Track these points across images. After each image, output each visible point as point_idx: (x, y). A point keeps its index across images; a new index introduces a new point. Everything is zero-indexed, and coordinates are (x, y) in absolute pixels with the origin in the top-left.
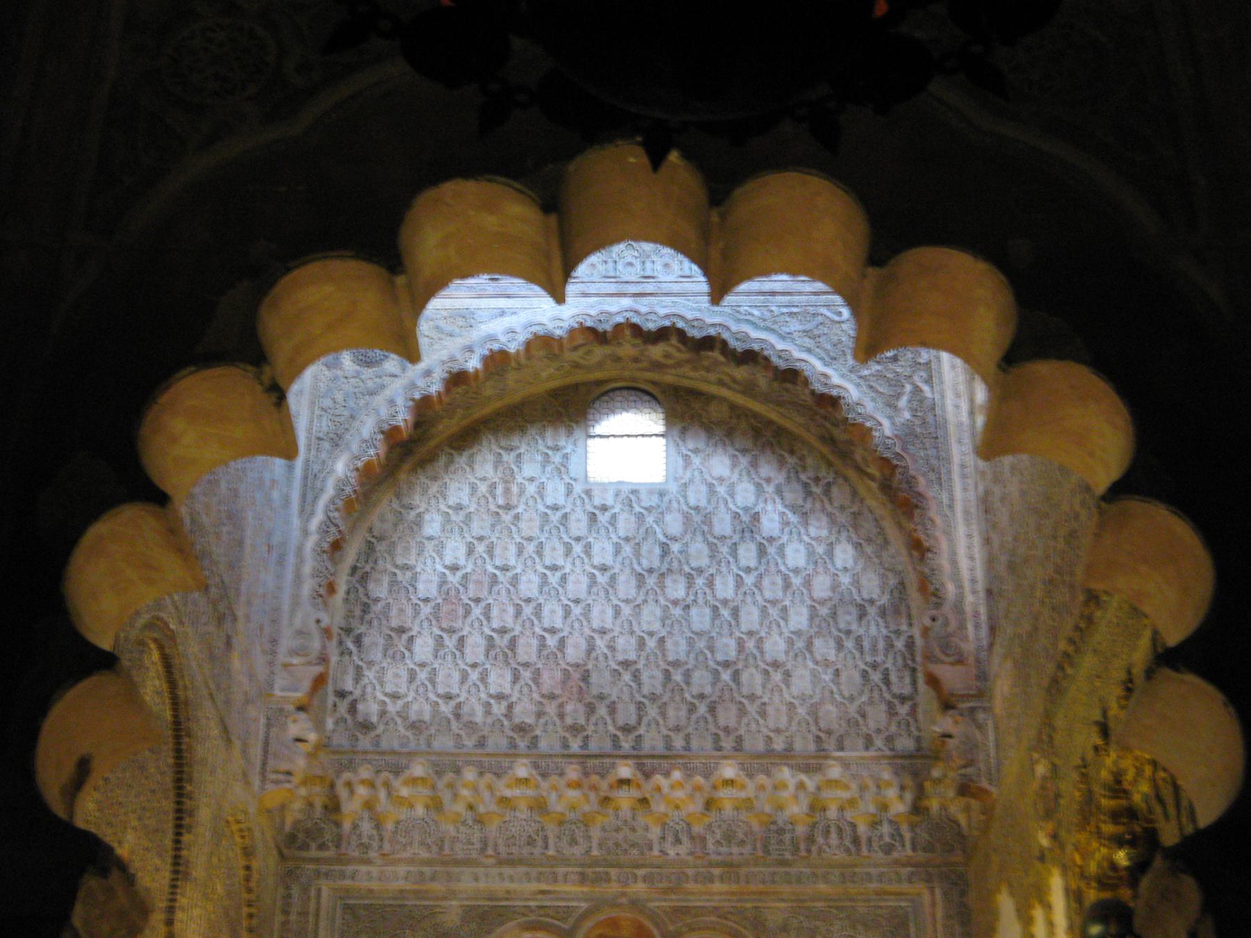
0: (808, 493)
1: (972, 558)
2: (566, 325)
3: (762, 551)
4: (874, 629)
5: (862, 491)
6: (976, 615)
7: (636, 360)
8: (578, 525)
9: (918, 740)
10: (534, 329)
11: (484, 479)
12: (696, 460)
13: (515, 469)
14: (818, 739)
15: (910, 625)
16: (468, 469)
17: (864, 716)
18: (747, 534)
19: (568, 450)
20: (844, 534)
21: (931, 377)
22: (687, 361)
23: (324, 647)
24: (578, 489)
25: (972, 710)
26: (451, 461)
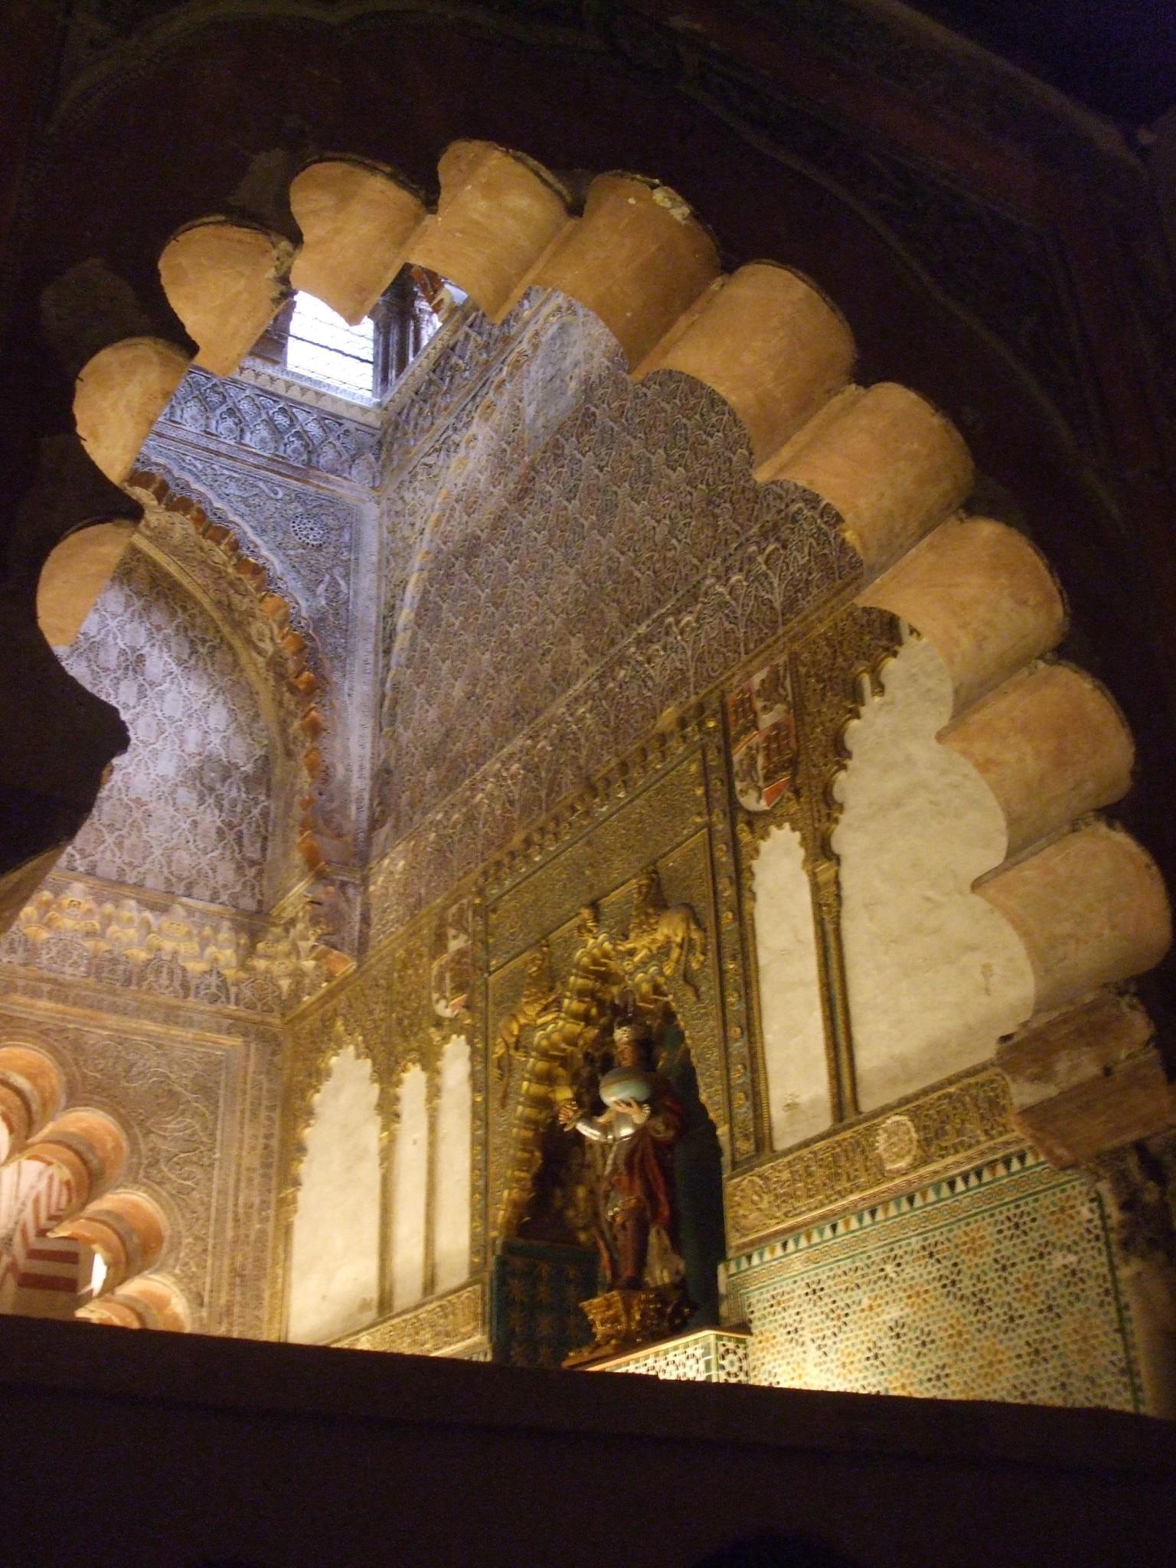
0: (194, 652)
1: (362, 746)
3: (142, 694)
4: (232, 792)
5: (244, 659)
6: (359, 800)
9: (260, 902)
14: (168, 880)
15: (268, 796)
17: (214, 870)
18: (130, 673)
20: (220, 698)
21: (348, 574)
25: (343, 885)
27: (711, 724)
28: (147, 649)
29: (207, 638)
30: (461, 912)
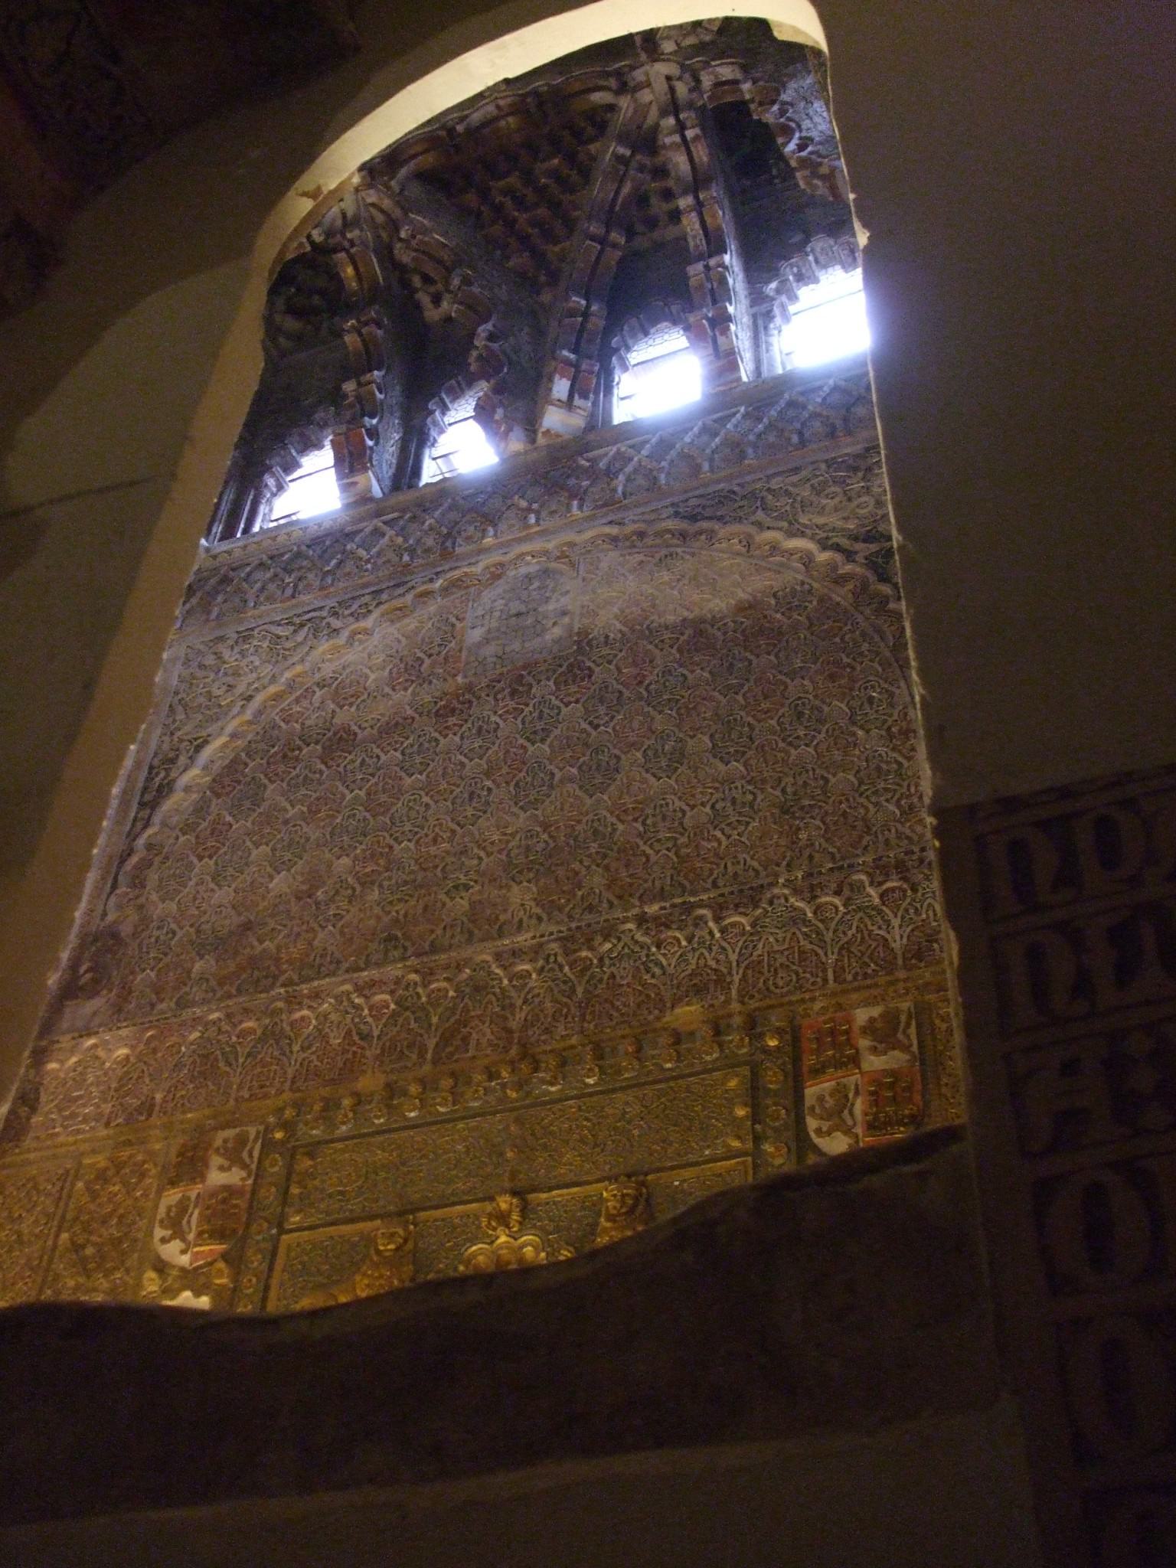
27: (773, 1043)
30: (242, 1141)
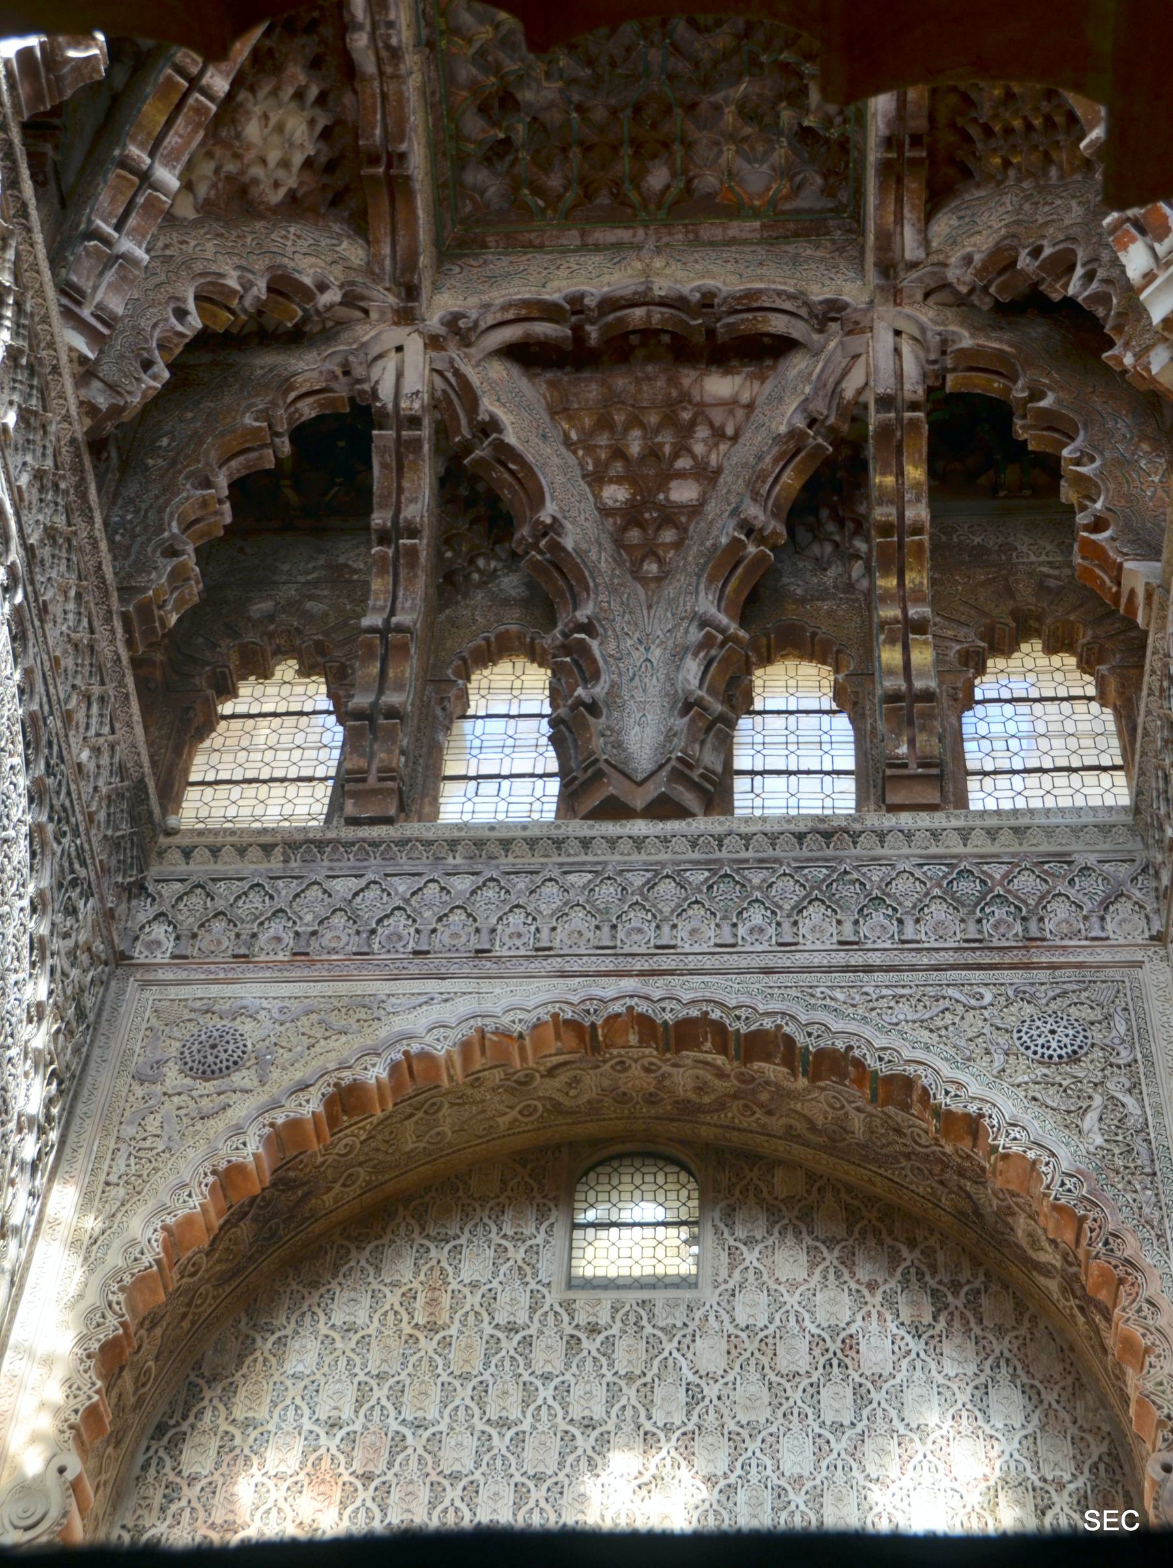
2: (531, 1017)
3: (861, 1397)
7: (651, 1099)
8: (548, 1355)
10: (479, 1022)
11: (395, 1284)
12: (751, 1257)
13: (450, 1270)
16: (372, 1271)
19: (539, 1240)
22: (735, 1096)
23: (65, 1514)
24: (551, 1299)
26: (344, 1256)
28: (859, 1322)
29: (963, 1281)
